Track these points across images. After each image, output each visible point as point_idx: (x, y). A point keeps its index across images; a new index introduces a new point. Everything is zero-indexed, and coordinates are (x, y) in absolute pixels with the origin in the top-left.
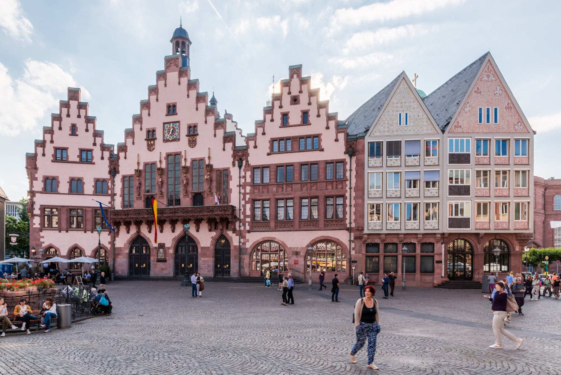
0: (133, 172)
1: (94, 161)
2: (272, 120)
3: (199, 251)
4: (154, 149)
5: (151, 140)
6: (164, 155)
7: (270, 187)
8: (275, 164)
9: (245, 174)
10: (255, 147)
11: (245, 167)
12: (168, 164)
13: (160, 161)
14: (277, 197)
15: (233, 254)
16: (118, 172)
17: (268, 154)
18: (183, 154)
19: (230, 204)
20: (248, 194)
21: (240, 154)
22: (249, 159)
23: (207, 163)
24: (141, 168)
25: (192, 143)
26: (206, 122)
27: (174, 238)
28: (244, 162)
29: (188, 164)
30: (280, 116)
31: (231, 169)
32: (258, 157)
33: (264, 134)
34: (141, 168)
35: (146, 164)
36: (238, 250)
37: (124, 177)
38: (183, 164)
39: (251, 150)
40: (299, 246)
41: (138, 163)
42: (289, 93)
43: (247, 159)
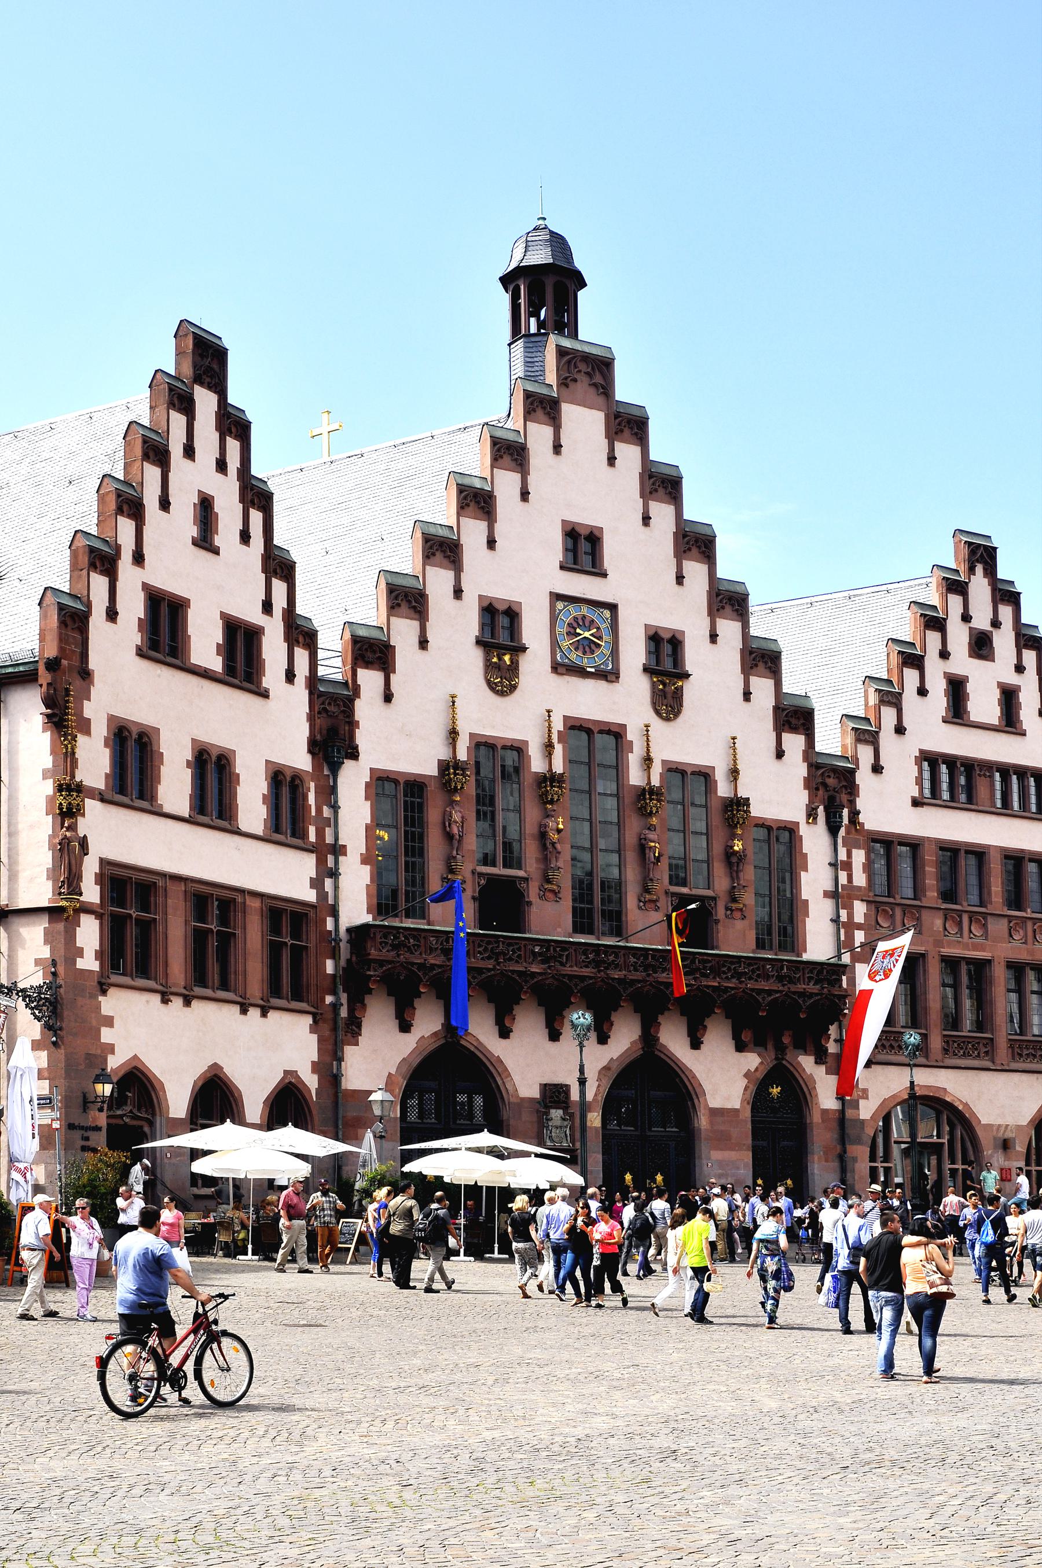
0: (432, 770)
1: (267, 682)
2: (922, 692)
3: (703, 1122)
4: (513, 688)
5: (503, 649)
6: (558, 725)
7: (926, 915)
8: (938, 841)
9: (849, 855)
10: (877, 769)
11: (848, 832)
12: (570, 761)
13: (549, 747)
14: (947, 951)
15: (821, 1138)
16: (354, 755)
17: (916, 803)
18: (633, 735)
19: (805, 957)
20: (859, 927)
21: (831, 782)
22: (860, 804)
23: (723, 790)
24: (462, 755)
25: (668, 702)
26: (713, 637)
27: (607, 1068)
28: (845, 812)
29: (656, 781)
30: (942, 684)
31: (804, 830)
32: (888, 803)
33: (900, 730)
34: (462, 755)
35: (482, 745)
36: (835, 1125)
37: (382, 783)
38: (635, 777)
39: (864, 777)
40: (1010, 1120)
41: (453, 734)
42: (966, 618)
43: (852, 803)
